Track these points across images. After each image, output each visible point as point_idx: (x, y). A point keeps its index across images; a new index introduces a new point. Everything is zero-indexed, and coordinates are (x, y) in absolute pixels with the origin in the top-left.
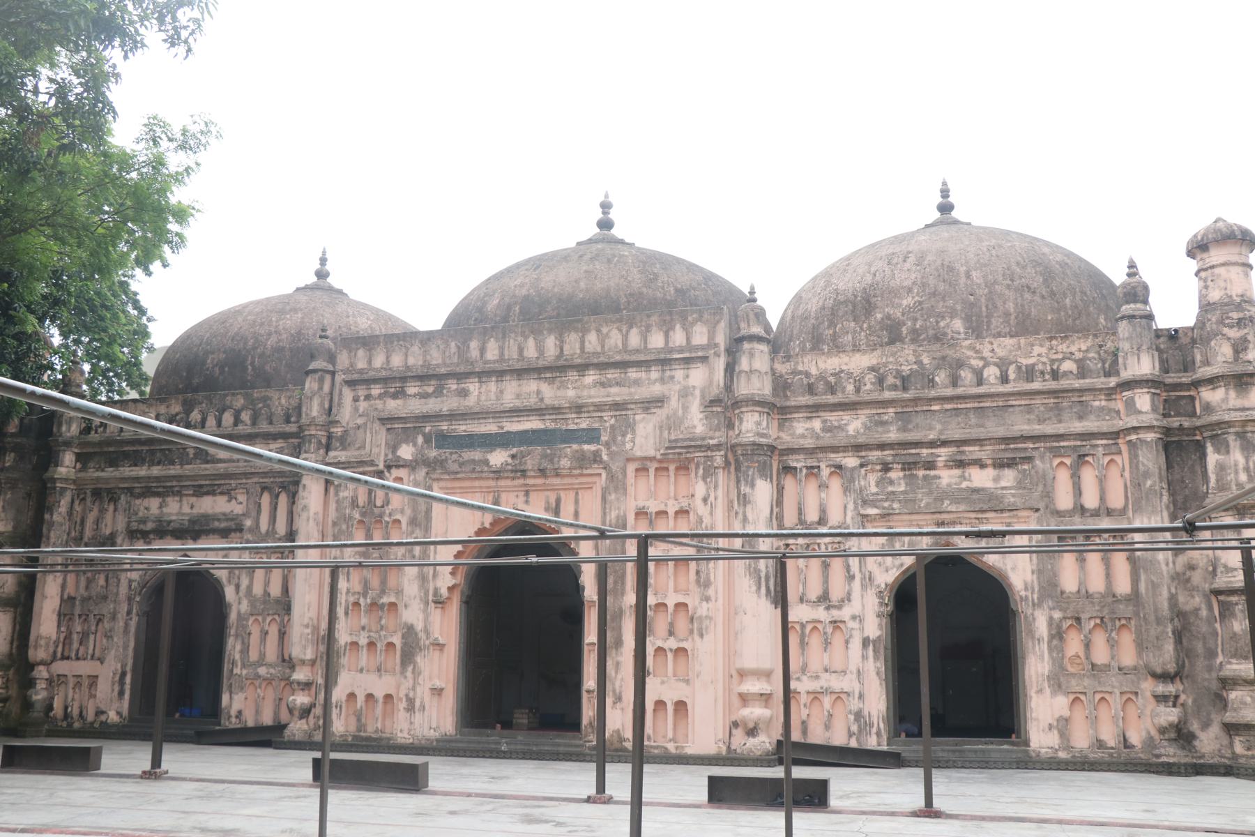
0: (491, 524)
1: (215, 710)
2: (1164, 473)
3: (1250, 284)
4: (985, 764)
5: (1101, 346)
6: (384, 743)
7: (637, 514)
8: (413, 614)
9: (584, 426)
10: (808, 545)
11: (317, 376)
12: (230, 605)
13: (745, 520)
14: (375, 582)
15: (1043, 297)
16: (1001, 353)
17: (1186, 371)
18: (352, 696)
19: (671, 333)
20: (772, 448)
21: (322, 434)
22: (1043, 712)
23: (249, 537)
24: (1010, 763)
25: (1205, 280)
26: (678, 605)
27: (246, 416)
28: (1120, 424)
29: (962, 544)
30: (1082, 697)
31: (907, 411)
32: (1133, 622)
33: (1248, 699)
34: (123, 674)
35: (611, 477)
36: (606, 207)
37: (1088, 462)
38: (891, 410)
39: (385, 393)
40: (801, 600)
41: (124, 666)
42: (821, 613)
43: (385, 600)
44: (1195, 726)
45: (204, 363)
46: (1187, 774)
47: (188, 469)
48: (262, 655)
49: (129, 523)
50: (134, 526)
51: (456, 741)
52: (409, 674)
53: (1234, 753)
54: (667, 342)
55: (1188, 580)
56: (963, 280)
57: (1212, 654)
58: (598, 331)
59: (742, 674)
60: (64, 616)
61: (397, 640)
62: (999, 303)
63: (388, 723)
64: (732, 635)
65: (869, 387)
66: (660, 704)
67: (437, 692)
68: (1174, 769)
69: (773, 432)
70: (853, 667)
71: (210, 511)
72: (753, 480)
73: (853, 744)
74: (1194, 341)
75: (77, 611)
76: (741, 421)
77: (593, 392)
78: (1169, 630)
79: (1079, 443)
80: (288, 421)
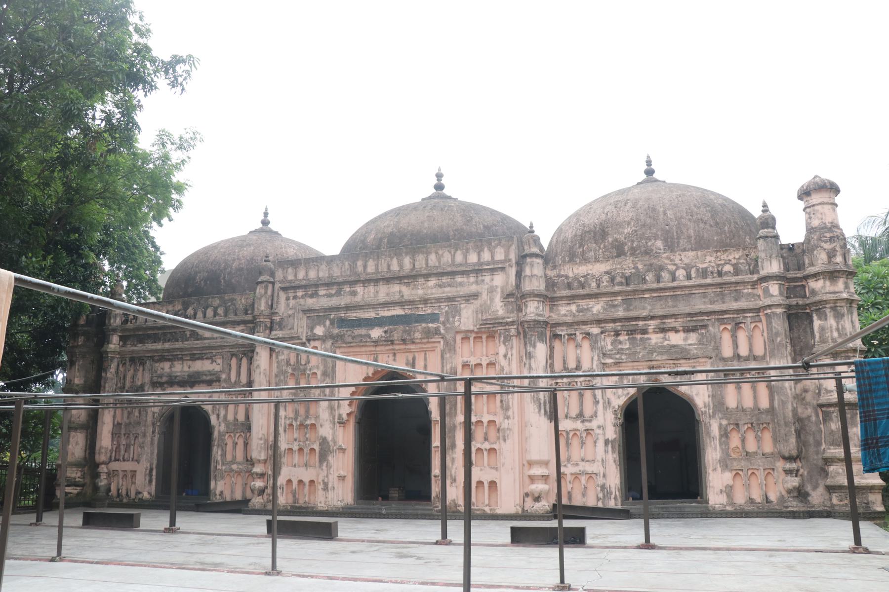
1: (206, 491)
2: (788, 333)
3: (836, 215)
4: (681, 515)
5: (747, 256)
6: (310, 510)
7: (463, 366)
8: (326, 431)
9: (429, 312)
10: (570, 383)
11: (263, 285)
12: (214, 427)
13: (530, 368)
14: (302, 411)
15: (711, 226)
16: (686, 261)
17: (799, 270)
18: (289, 481)
20: (546, 323)
22: (717, 482)
23: (224, 385)
24: (697, 514)
25: (809, 214)
26: (489, 422)
27: (220, 311)
28: (760, 303)
29: (665, 380)
30: (740, 473)
31: (629, 298)
32: (771, 426)
33: (841, 471)
34: (151, 470)
35: (447, 343)
36: (439, 176)
38: (619, 298)
39: (306, 294)
40: (566, 417)
41: (151, 464)
42: (578, 425)
43: (308, 422)
44: (809, 488)
45: (194, 279)
46: (804, 518)
47: (186, 344)
48: (234, 457)
49: (152, 378)
50: (155, 379)
51: (354, 508)
52: (324, 467)
53: (832, 504)
54: (479, 259)
55: (804, 399)
56: (661, 216)
57: (818, 444)
58: (437, 253)
59: (531, 464)
60: (115, 435)
61: (316, 447)
62: (684, 230)
63: (312, 498)
64: (524, 439)
65: (605, 284)
66: (480, 483)
67: (342, 478)
68: (796, 515)
69: (547, 313)
70: (599, 458)
71: (200, 370)
72: (535, 343)
73: (600, 505)
74: (804, 251)
75: (123, 432)
76: (526, 306)
77: (434, 291)
78: (793, 430)
80: (246, 313)
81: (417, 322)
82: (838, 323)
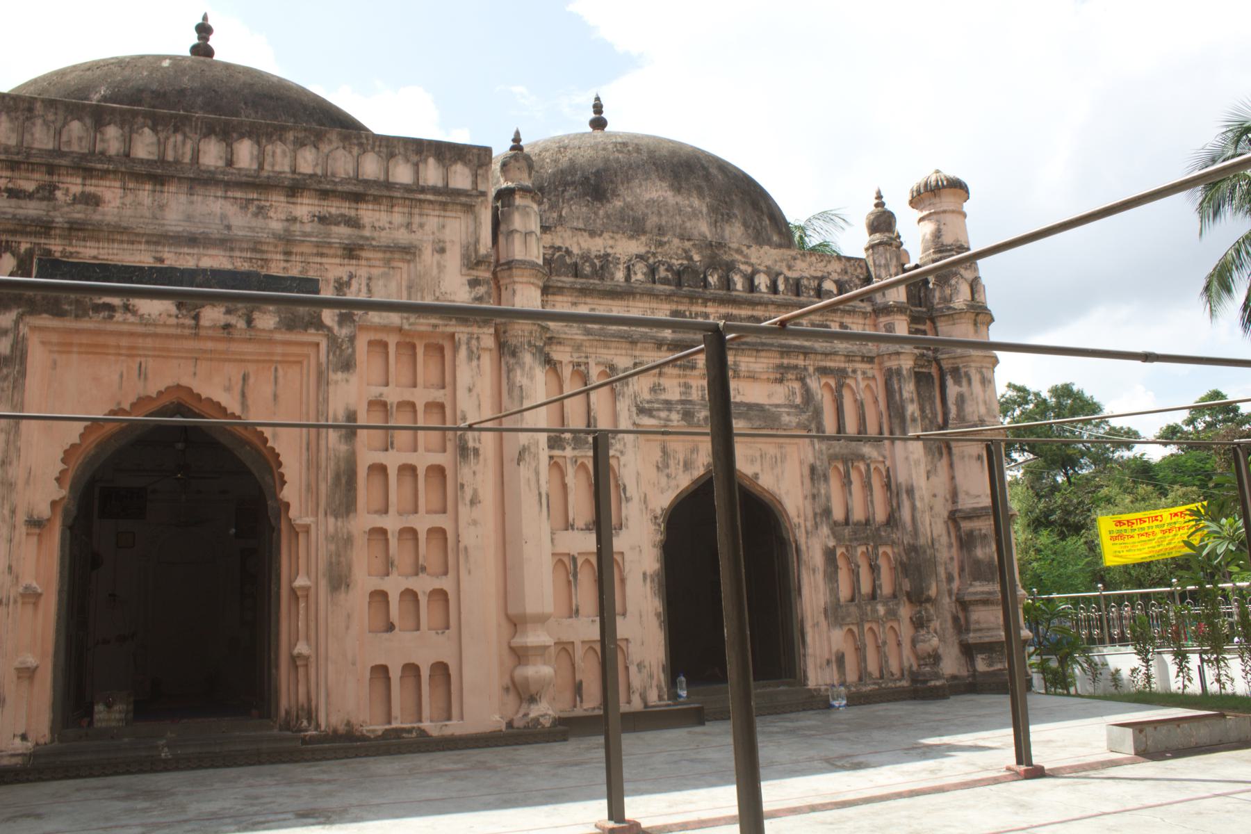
0: (133, 405)
9: (295, 272)
19: (421, 166)
22: (823, 646)
26: (431, 531)
36: (204, 30)
37: (849, 386)
59: (516, 622)
66: (412, 670)
79: (842, 365)
82: (984, 391)
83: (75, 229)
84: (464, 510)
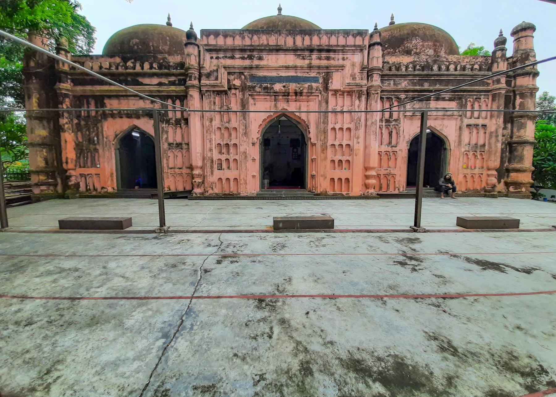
9: (312, 75)
21: (197, 74)
65: (410, 69)
66: (340, 179)
81: (304, 81)
83: (258, 67)
84: (355, 140)
